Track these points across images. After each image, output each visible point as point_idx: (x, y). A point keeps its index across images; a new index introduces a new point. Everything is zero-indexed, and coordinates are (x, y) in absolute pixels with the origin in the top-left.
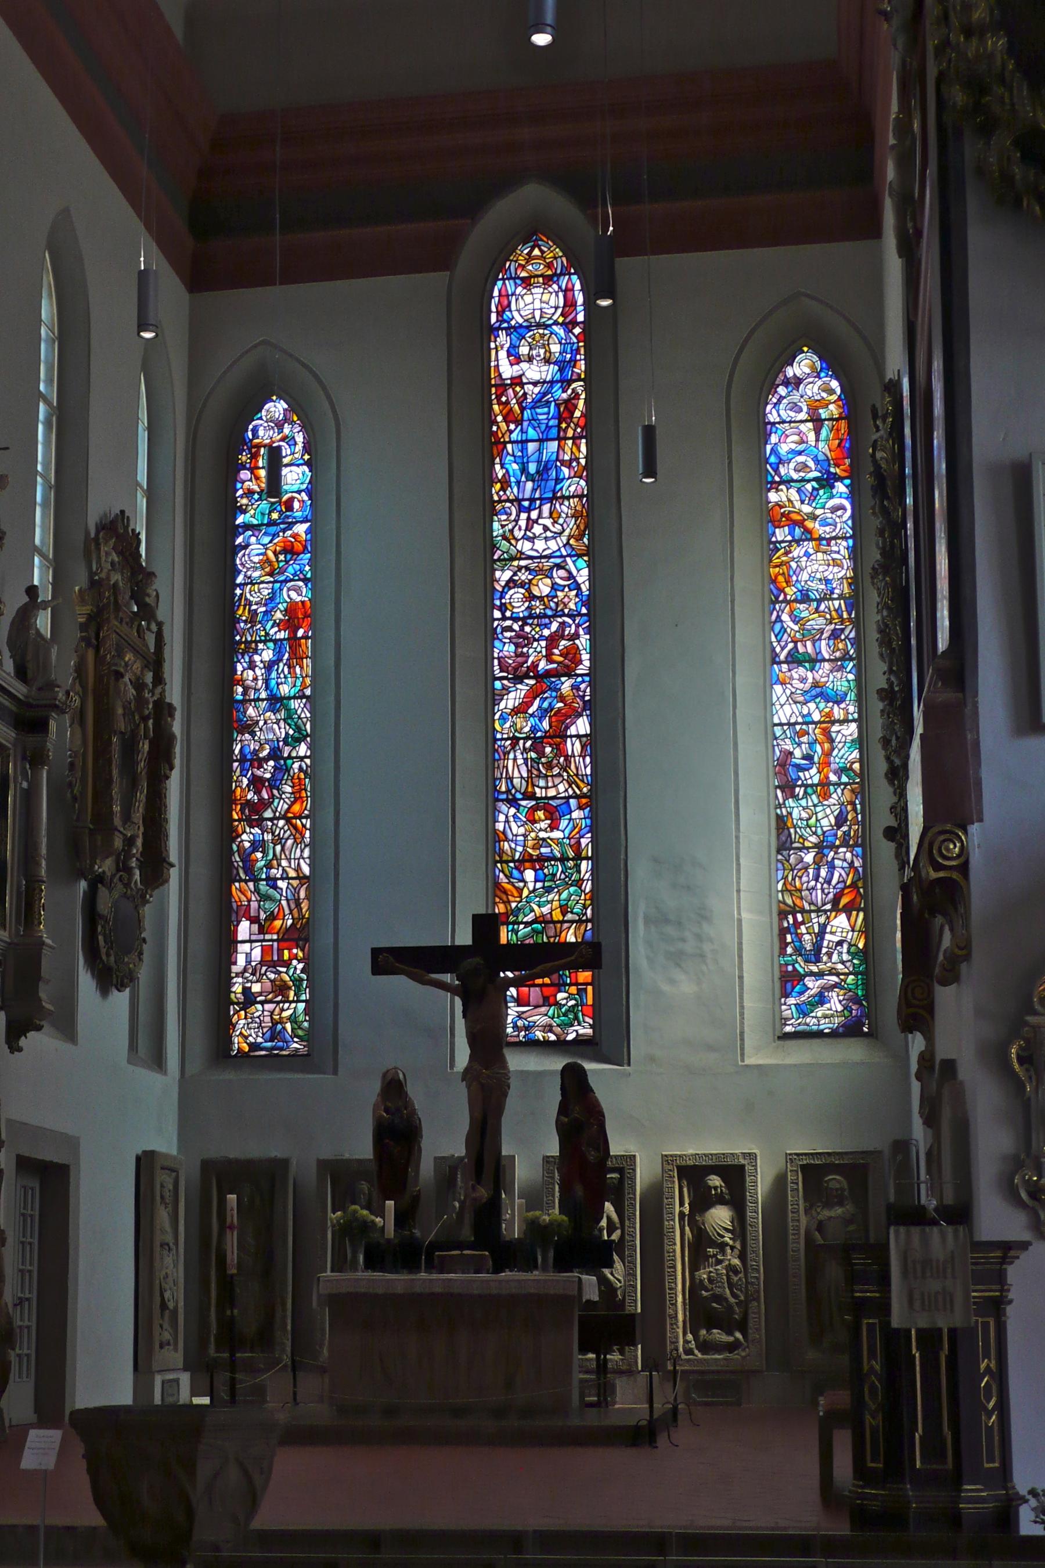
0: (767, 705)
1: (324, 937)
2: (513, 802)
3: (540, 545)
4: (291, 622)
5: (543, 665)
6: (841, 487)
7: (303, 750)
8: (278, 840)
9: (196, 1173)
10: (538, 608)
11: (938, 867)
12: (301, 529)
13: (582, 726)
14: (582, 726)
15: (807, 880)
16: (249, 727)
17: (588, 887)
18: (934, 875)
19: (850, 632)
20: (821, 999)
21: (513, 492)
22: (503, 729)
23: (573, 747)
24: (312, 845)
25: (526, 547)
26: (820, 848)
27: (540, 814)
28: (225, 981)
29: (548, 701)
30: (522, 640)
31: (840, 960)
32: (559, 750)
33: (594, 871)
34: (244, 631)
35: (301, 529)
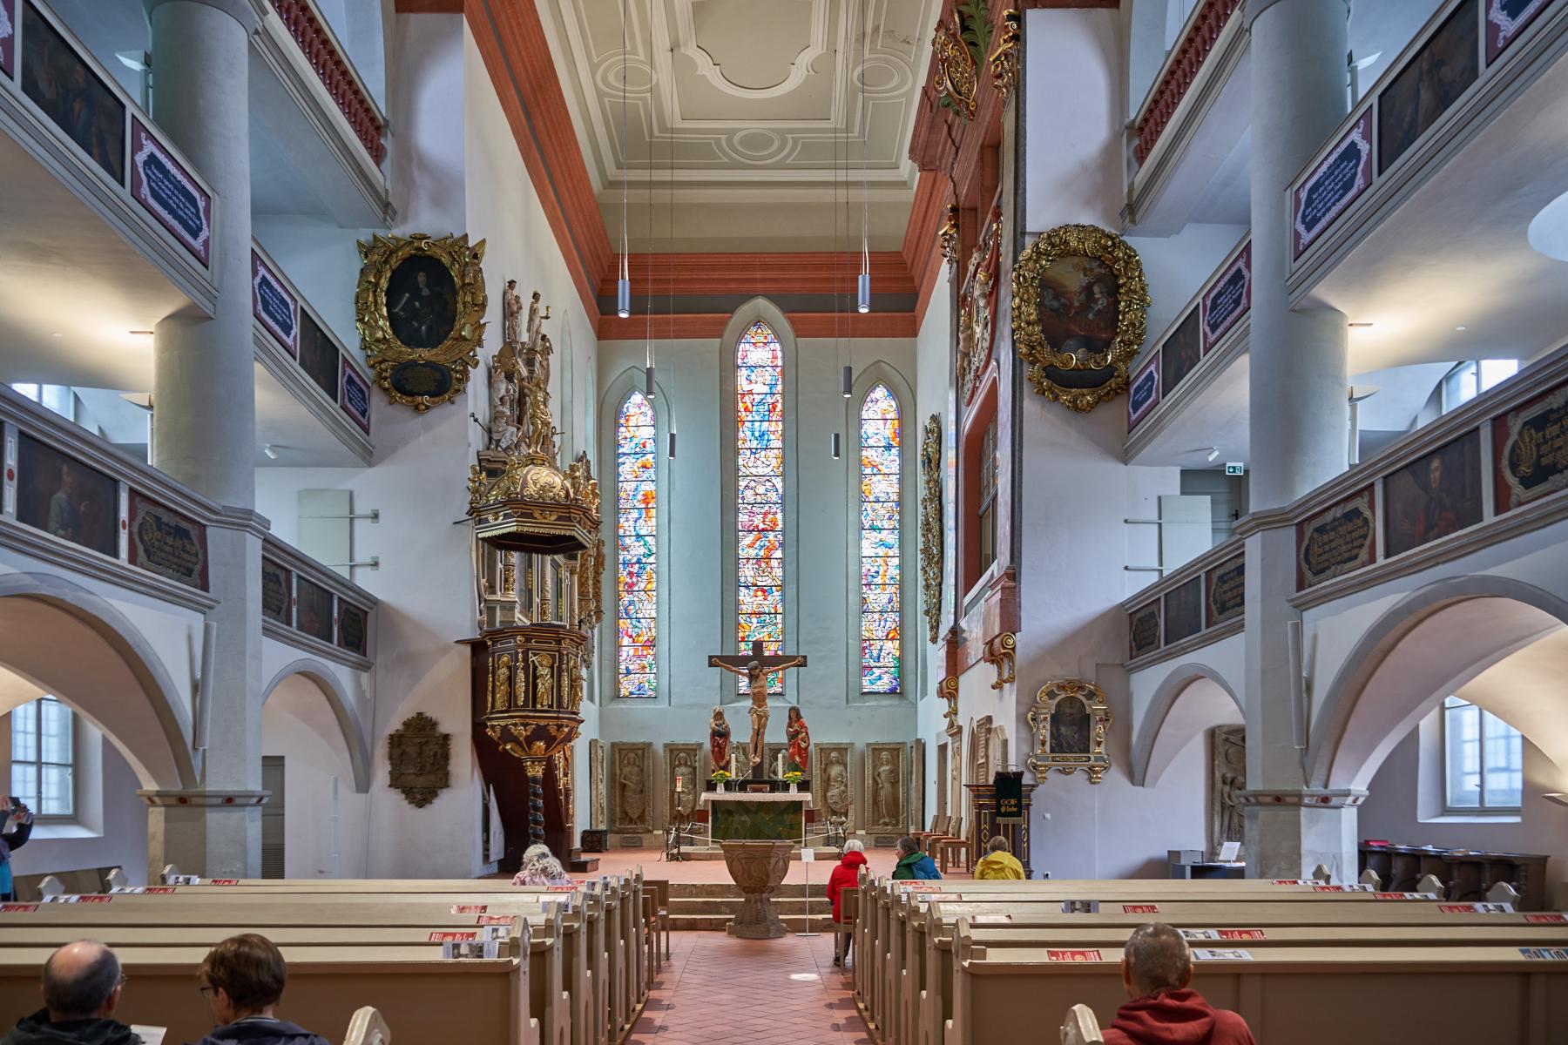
0: (860, 548)
1: (663, 646)
2: (747, 587)
3: (760, 471)
4: (646, 500)
5: (761, 526)
6: (894, 451)
7: (652, 559)
8: (641, 601)
9: (607, 748)
12: (650, 457)
14: (778, 554)
16: (626, 549)
19: (897, 517)
20: (880, 678)
23: (774, 563)
24: (657, 603)
25: (754, 471)
26: (881, 612)
28: (617, 663)
29: (764, 542)
31: (888, 661)
33: (784, 619)
34: (623, 504)
35: (650, 457)
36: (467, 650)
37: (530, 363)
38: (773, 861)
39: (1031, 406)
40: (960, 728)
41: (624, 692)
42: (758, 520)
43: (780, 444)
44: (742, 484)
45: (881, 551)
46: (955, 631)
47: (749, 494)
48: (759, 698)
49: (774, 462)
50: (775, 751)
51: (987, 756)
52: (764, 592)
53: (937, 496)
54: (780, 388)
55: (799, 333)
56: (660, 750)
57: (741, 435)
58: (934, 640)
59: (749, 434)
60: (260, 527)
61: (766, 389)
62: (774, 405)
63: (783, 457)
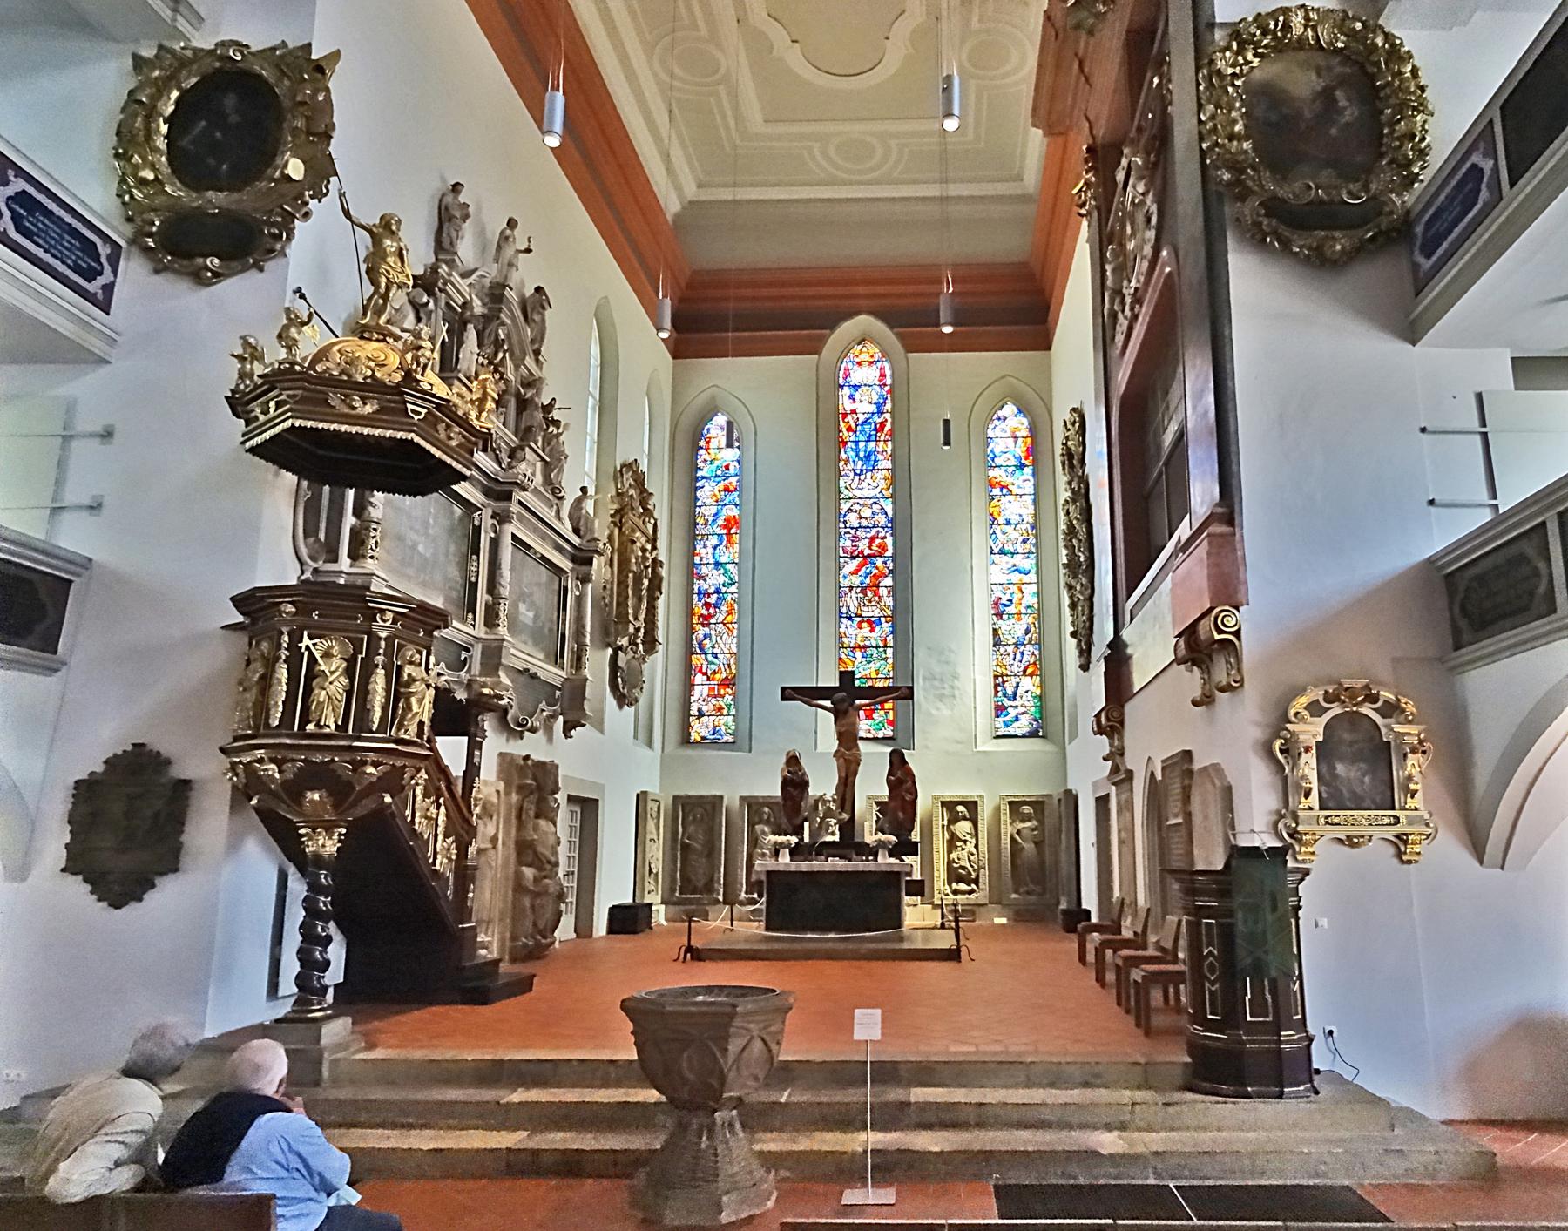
2: (850, 618)
5: (867, 552)
10: (864, 523)
11: (1220, 632)
13: (888, 581)
14: (888, 581)
15: (1009, 660)
17: (890, 661)
18: (1217, 637)
21: (850, 466)
22: (845, 583)
25: (858, 493)
27: (864, 625)
30: (856, 538)
32: (876, 594)
33: (894, 654)
38: (734, 1046)
40: (1130, 774)
42: (863, 545)
43: (889, 464)
44: (845, 507)
45: (1016, 577)
47: (853, 519)
49: (883, 484)
51: (1188, 816)
52: (869, 622)
53: (1081, 494)
54: (888, 406)
55: (910, 348)
57: (843, 456)
59: (852, 454)
61: (873, 408)
62: (882, 425)
63: (893, 476)
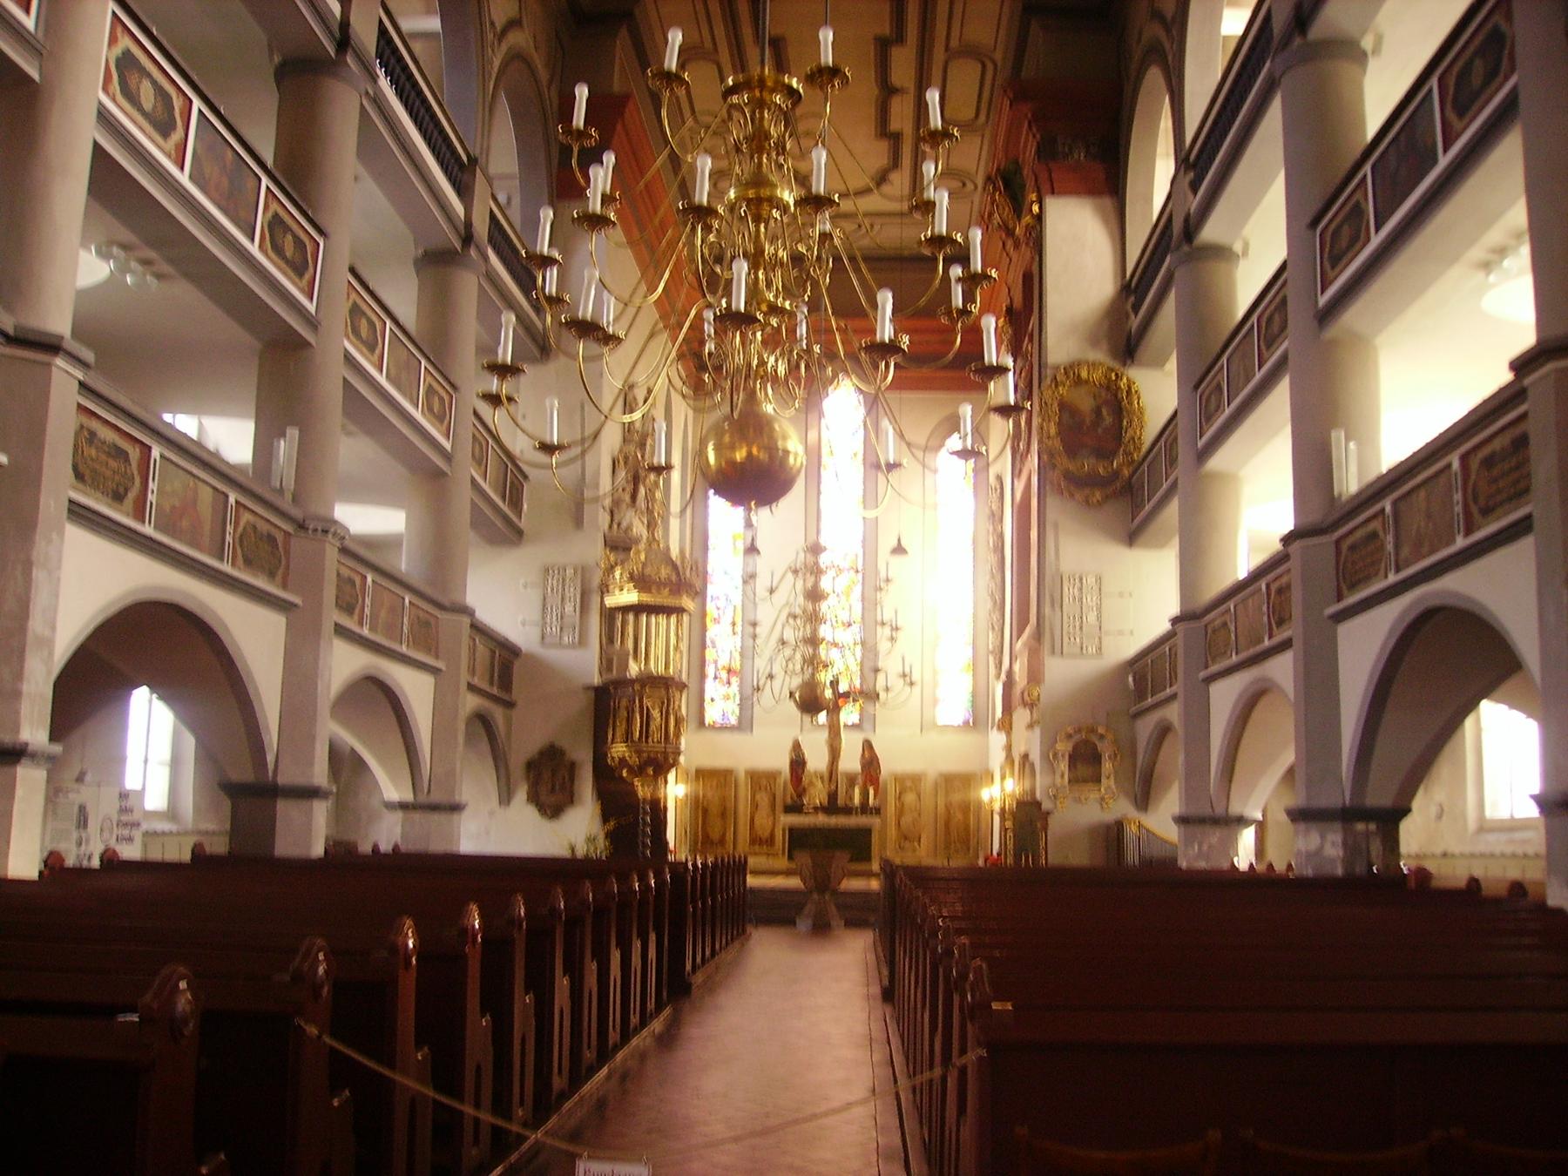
36: (592, 694)
37: (642, 445)
39: (1052, 502)
41: (708, 720)
46: (1010, 673)
48: (834, 730)
50: (851, 780)
56: (742, 776)
58: (998, 676)
60: (467, 611)
